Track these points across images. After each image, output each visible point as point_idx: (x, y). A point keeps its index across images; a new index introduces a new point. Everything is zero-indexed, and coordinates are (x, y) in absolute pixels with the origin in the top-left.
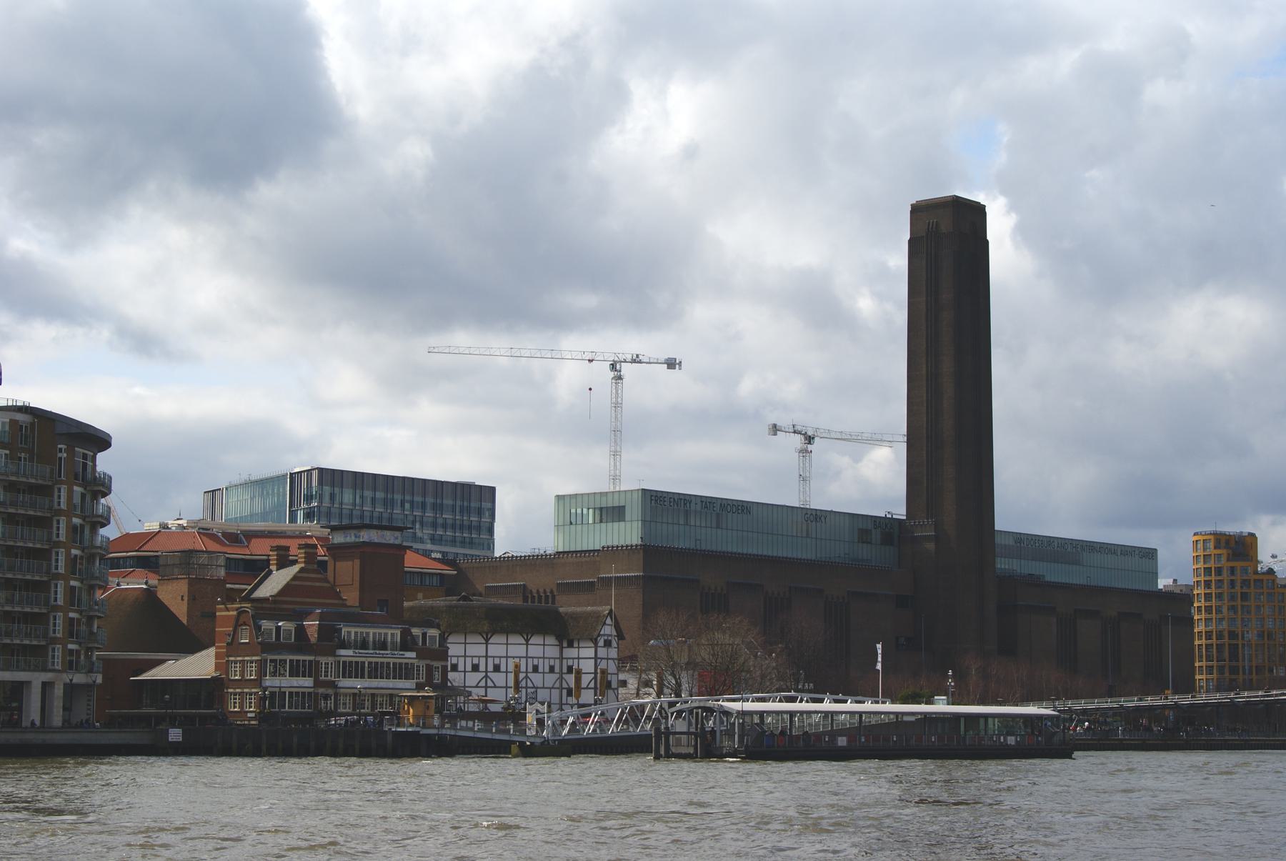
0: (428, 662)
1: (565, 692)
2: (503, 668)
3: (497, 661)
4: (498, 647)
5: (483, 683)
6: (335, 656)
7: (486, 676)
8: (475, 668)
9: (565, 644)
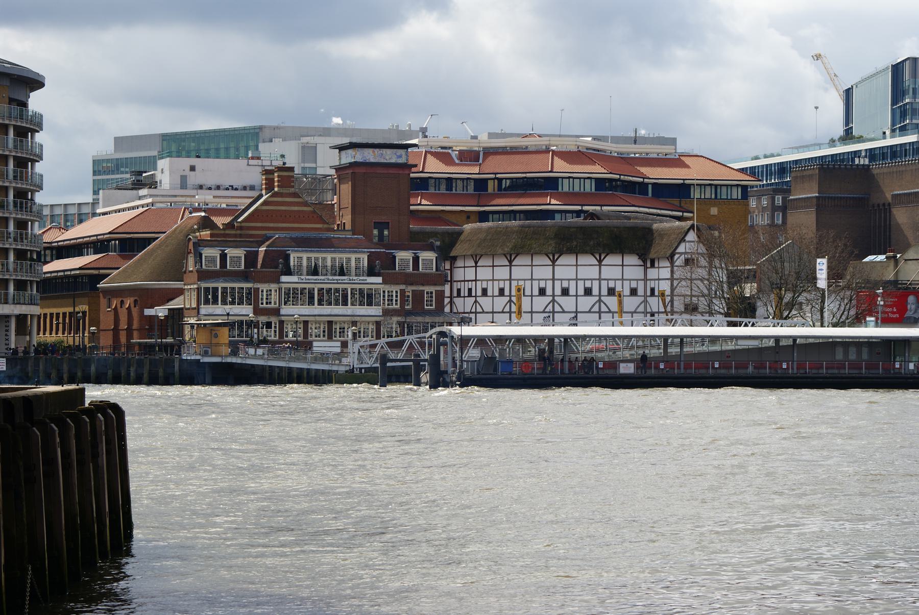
0: (403, 287)
2: (572, 291)
3: (565, 284)
4: (521, 271)
5: (550, 308)
6: (278, 282)
8: (542, 292)
9: (649, 265)
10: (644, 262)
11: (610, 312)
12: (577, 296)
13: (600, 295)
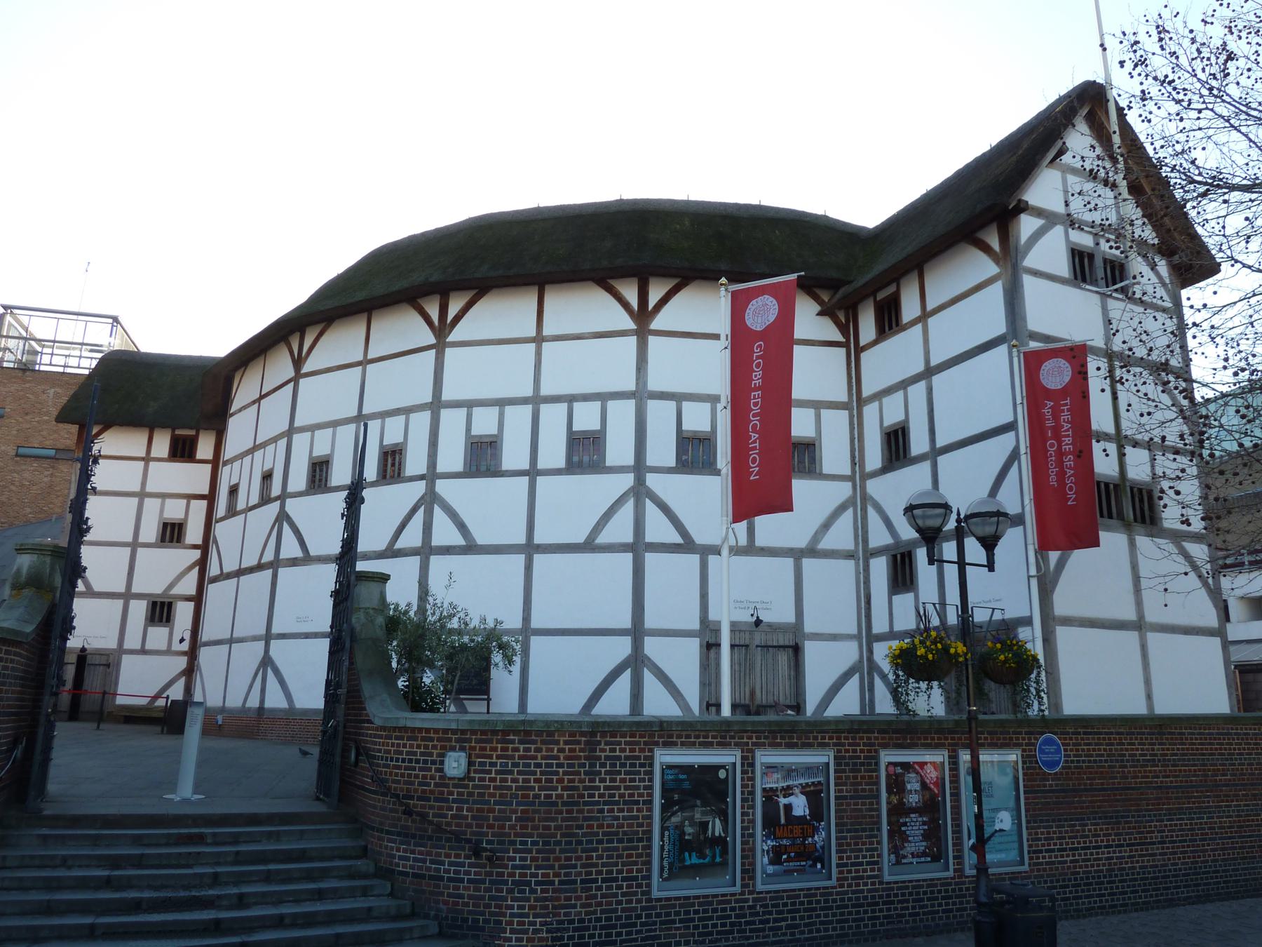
1: (880, 568)
2: (514, 455)
3: (485, 423)
5: (412, 537)
7: (430, 500)
10: (843, 329)
11: (687, 545)
12: (533, 473)
13: (640, 468)
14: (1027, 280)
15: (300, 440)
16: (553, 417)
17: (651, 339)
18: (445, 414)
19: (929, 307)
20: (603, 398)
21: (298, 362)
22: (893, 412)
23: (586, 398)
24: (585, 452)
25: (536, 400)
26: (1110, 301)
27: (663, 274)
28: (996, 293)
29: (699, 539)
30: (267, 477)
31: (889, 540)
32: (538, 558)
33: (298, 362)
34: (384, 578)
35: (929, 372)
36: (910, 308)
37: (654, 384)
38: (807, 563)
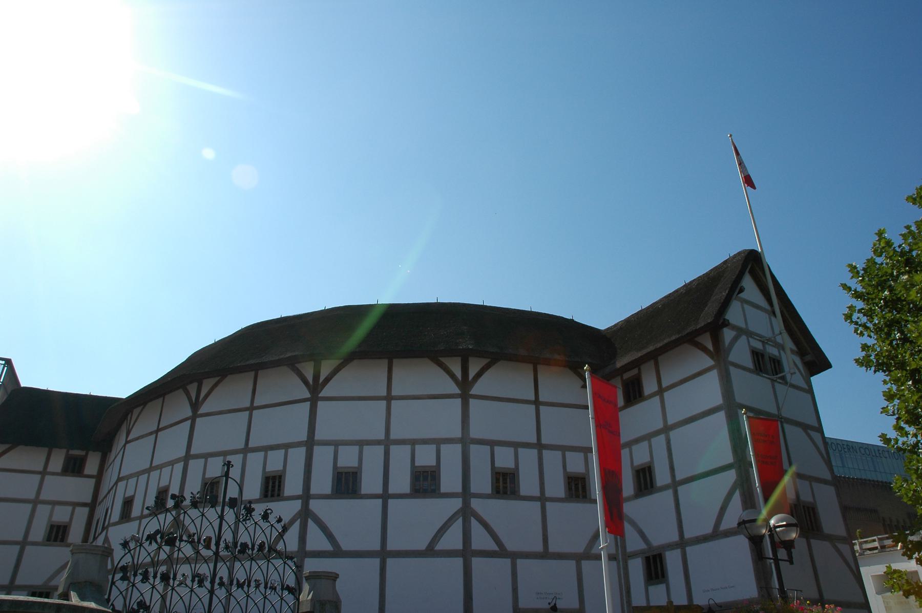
1: (637, 568)
2: (370, 482)
3: (348, 458)
11: (502, 552)
12: (385, 496)
13: (466, 493)
14: (732, 369)
15: (196, 466)
16: (400, 456)
17: (472, 401)
18: (317, 449)
19: (664, 385)
20: (438, 442)
21: (195, 406)
22: (640, 455)
23: (425, 442)
24: (425, 483)
25: (387, 443)
26: (776, 384)
27: (480, 354)
28: (713, 379)
29: (511, 546)
30: (162, 495)
31: (643, 546)
32: (390, 562)
33: (195, 406)
34: (334, 577)
35: (667, 429)
36: (649, 385)
37: (474, 433)
38: (583, 562)
